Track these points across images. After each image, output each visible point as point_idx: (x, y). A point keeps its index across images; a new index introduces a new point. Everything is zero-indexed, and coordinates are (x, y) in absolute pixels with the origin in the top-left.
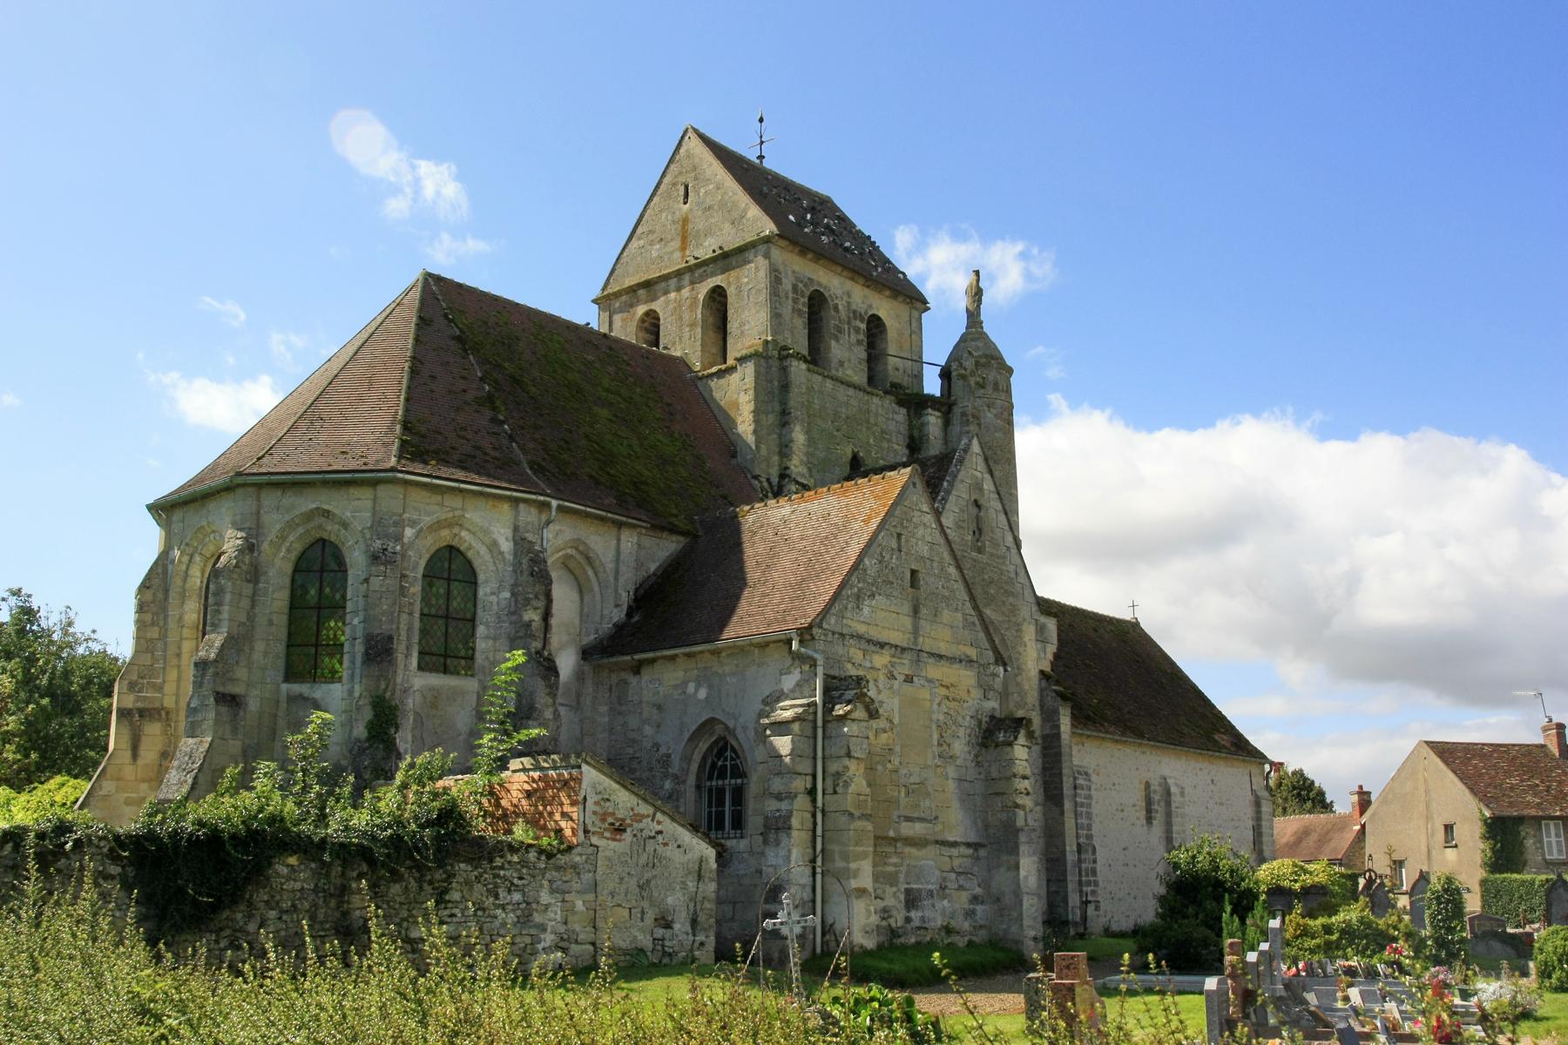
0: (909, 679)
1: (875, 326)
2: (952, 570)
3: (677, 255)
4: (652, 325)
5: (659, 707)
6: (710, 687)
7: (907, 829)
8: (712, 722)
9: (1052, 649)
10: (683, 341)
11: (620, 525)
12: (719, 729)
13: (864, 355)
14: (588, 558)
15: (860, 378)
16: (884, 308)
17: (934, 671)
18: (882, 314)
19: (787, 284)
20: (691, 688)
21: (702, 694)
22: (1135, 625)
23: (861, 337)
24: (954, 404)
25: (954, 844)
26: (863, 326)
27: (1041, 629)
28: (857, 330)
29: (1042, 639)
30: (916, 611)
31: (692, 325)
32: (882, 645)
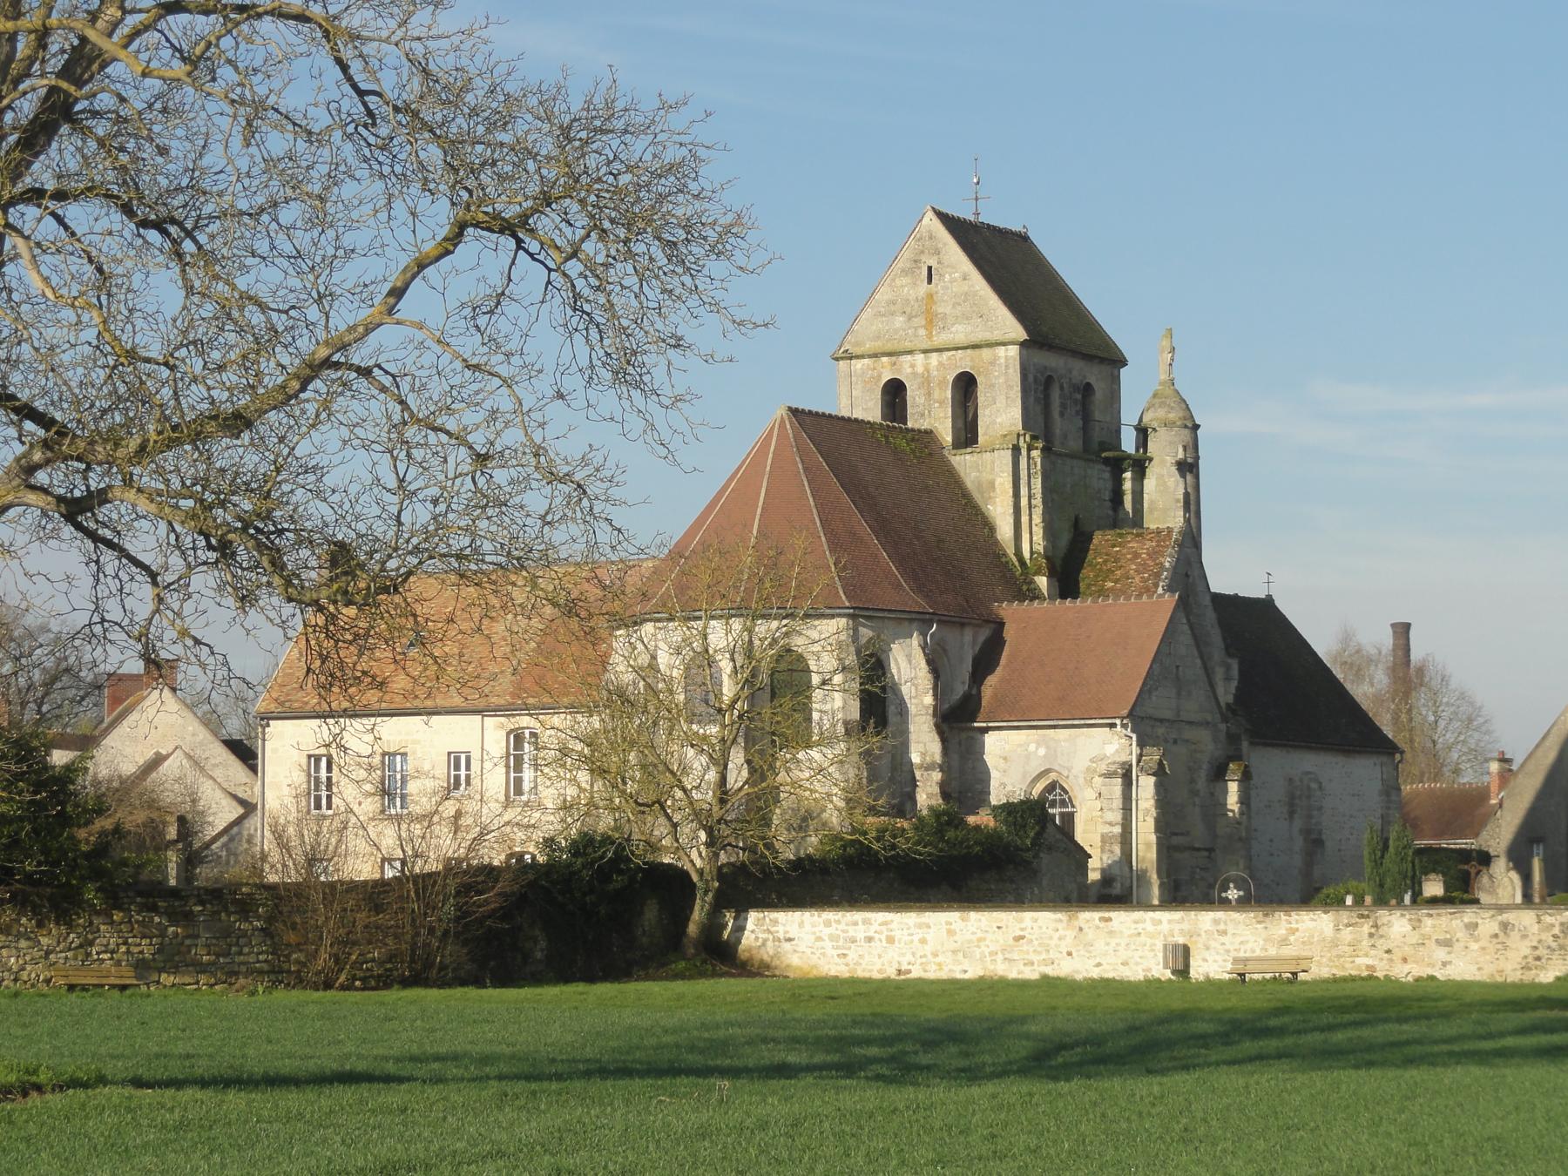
0: (1175, 742)
1: (1088, 389)
2: (1198, 661)
3: (922, 332)
4: (895, 392)
5: (1005, 759)
6: (1048, 747)
7: (1176, 840)
8: (1047, 771)
9: (1235, 683)
10: (932, 413)
11: (963, 625)
12: (1053, 776)
13: (1080, 423)
14: (945, 651)
15: (1075, 444)
16: (1094, 375)
17: (1190, 733)
18: (1092, 380)
19: (1031, 378)
20: (1032, 747)
21: (1042, 752)
22: (1267, 605)
23: (1079, 407)
24: (1151, 460)
25: (1198, 850)
26: (1079, 397)
27: (1228, 668)
28: (1076, 402)
29: (1228, 679)
30: (1179, 694)
31: (941, 403)
32: (1161, 721)
